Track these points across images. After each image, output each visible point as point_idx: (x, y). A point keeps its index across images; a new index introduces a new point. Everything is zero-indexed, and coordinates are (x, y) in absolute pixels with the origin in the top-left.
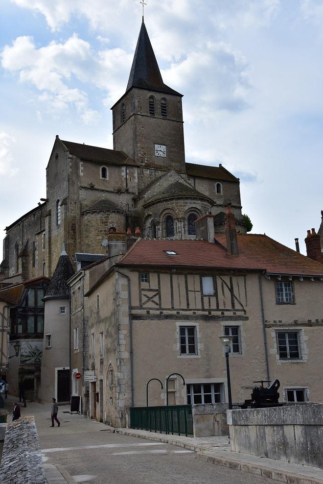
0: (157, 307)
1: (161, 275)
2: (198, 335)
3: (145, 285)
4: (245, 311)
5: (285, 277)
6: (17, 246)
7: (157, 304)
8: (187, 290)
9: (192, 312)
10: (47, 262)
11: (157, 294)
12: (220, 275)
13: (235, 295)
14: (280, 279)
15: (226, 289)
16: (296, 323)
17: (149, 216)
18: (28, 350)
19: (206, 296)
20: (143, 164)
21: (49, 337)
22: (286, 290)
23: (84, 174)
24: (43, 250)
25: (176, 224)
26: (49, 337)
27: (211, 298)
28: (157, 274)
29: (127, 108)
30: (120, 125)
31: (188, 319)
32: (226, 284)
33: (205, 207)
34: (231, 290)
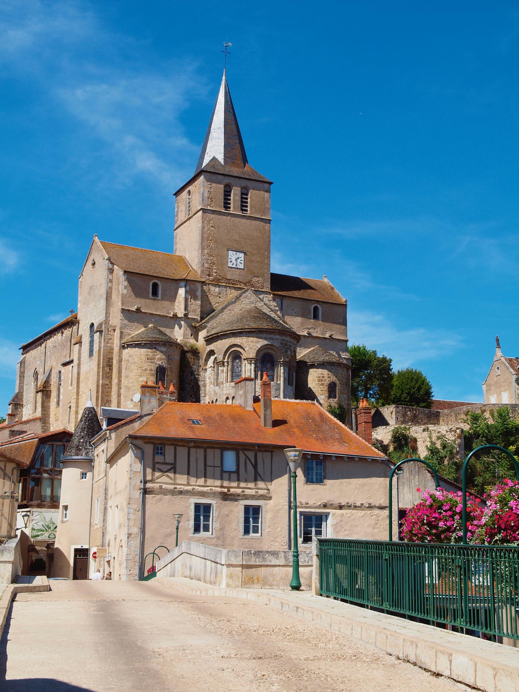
0: (171, 482)
1: (177, 448)
2: (214, 513)
3: (159, 458)
4: (268, 490)
5: (315, 457)
6: (36, 374)
7: (171, 479)
8: (205, 465)
9: (209, 488)
10: (73, 405)
11: (172, 468)
12: (243, 450)
13: (259, 472)
14: (309, 457)
15: (250, 466)
16: (325, 506)
17: (212, 353)
18: (40, 524)
19: (226, 472)
20: (211, 278)
21: (66, 508)
22: (317, 470)
23: (127, 292)
24: (70, 388)
25: (245, 365)
26: (66, 508)
27: (232, 474)
28: (173, 447)
29: (194, 197)
30: (184, 219)
31: (204, 496)
32: (249, 459)
33: (286, 344)
34: (255, 467)
